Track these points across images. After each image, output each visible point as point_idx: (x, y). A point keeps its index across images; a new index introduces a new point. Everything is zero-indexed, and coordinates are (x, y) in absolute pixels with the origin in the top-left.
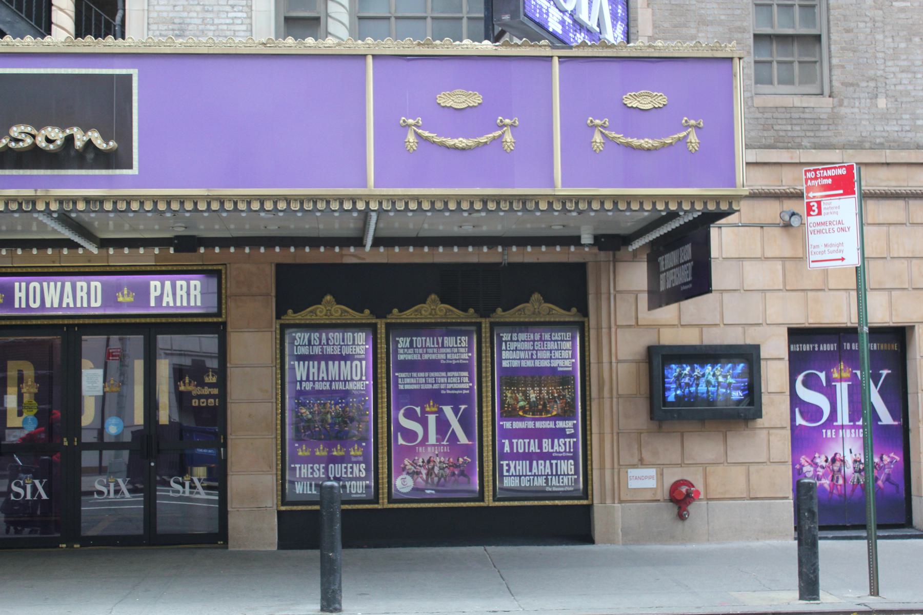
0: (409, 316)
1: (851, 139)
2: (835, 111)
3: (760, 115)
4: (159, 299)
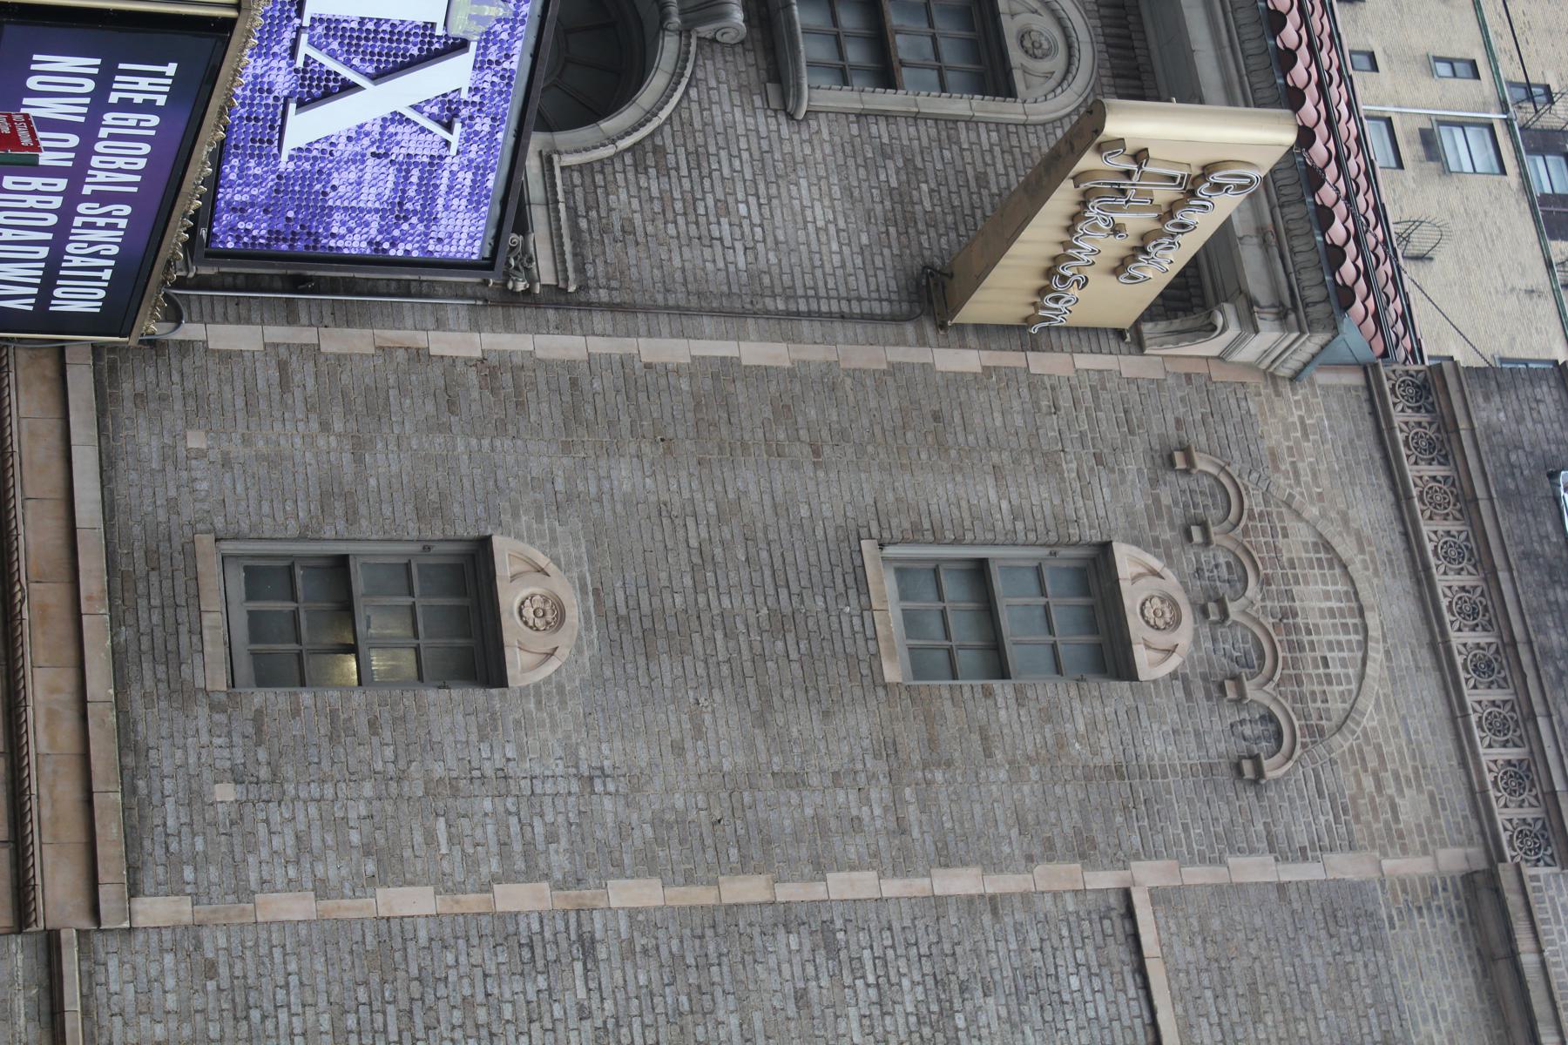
1: (141, 727)
2: (200, 696)
3: (177, 545)
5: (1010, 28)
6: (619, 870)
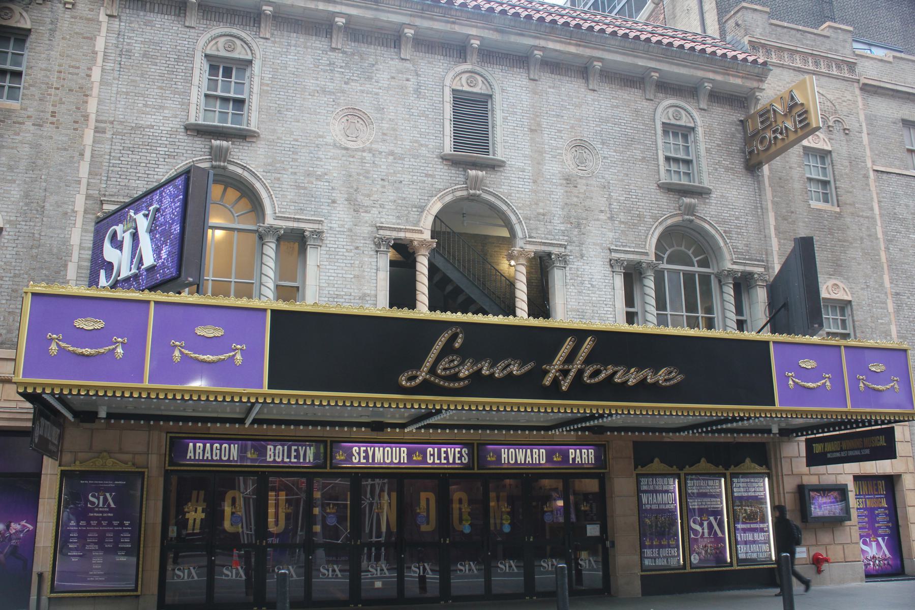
0: (693, 469)
4: (574, 459)
5: (673, 122)
6: (883, 283)
